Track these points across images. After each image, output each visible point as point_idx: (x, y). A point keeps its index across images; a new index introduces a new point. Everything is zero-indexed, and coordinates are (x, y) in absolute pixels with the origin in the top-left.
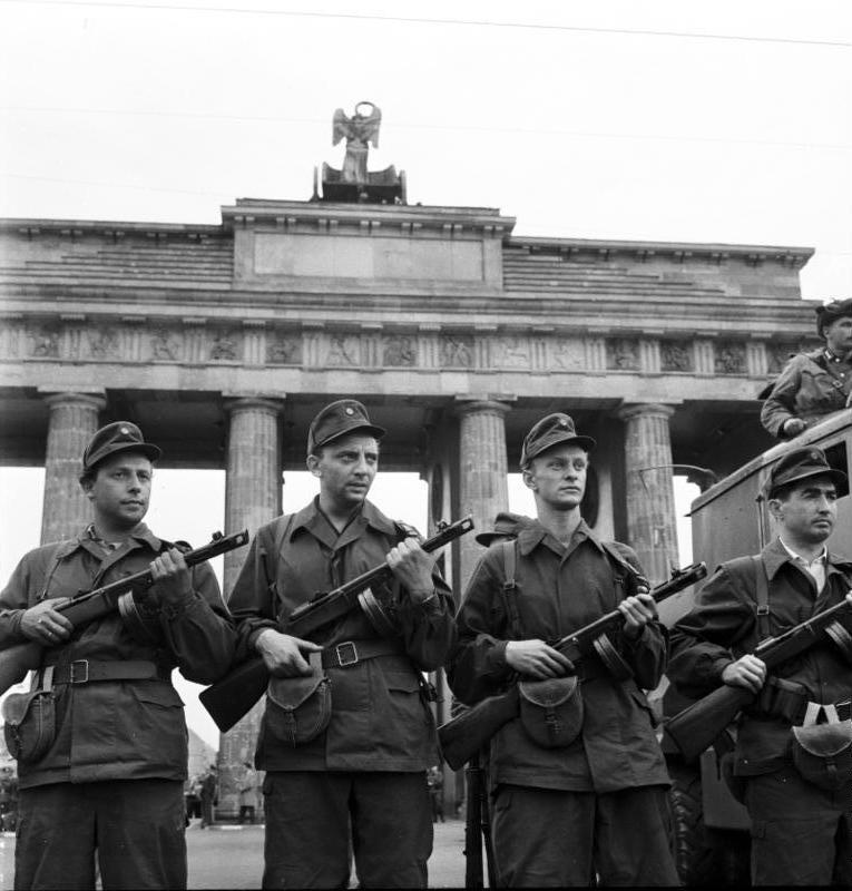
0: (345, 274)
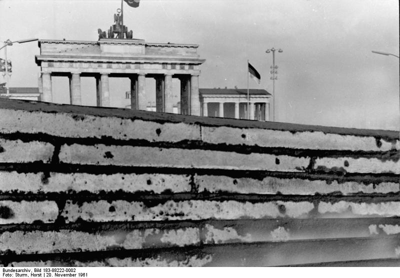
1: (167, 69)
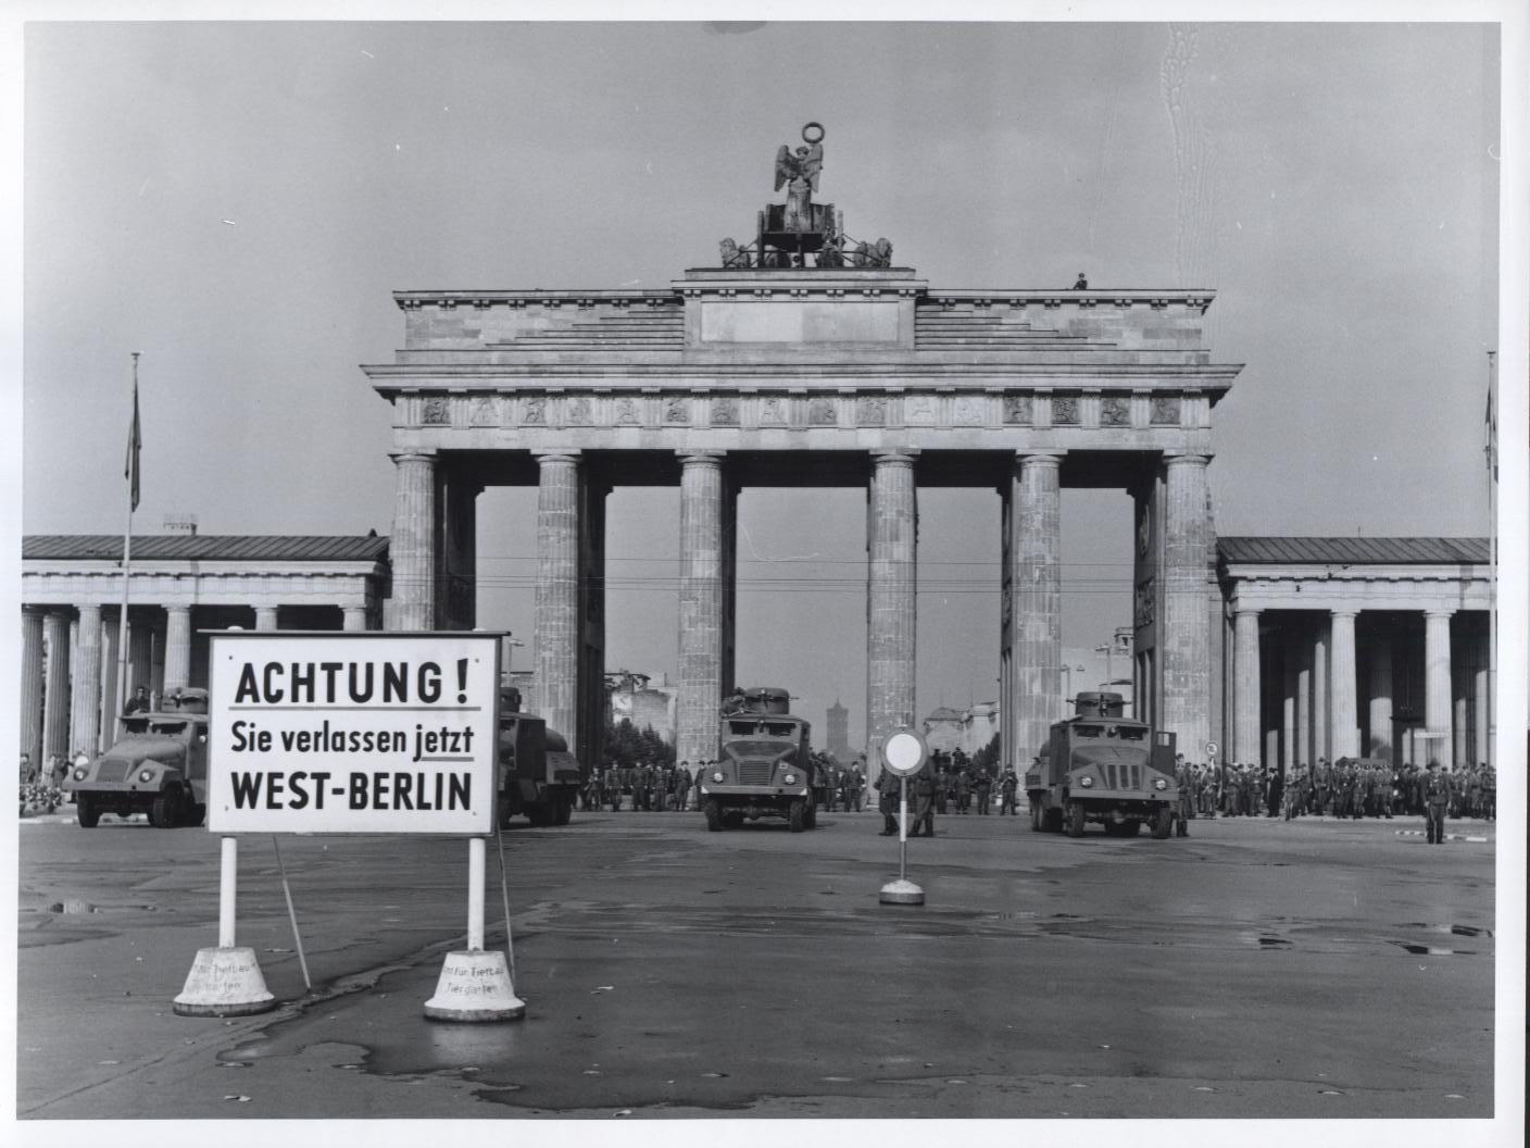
0: (777, 339)
1: (1029, 425)
